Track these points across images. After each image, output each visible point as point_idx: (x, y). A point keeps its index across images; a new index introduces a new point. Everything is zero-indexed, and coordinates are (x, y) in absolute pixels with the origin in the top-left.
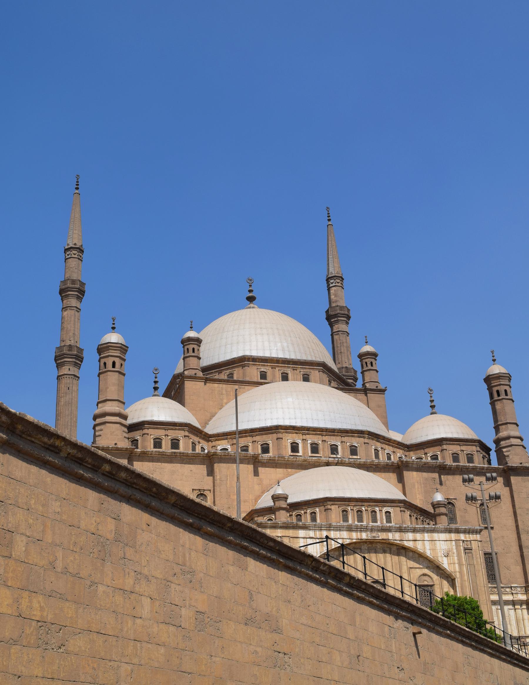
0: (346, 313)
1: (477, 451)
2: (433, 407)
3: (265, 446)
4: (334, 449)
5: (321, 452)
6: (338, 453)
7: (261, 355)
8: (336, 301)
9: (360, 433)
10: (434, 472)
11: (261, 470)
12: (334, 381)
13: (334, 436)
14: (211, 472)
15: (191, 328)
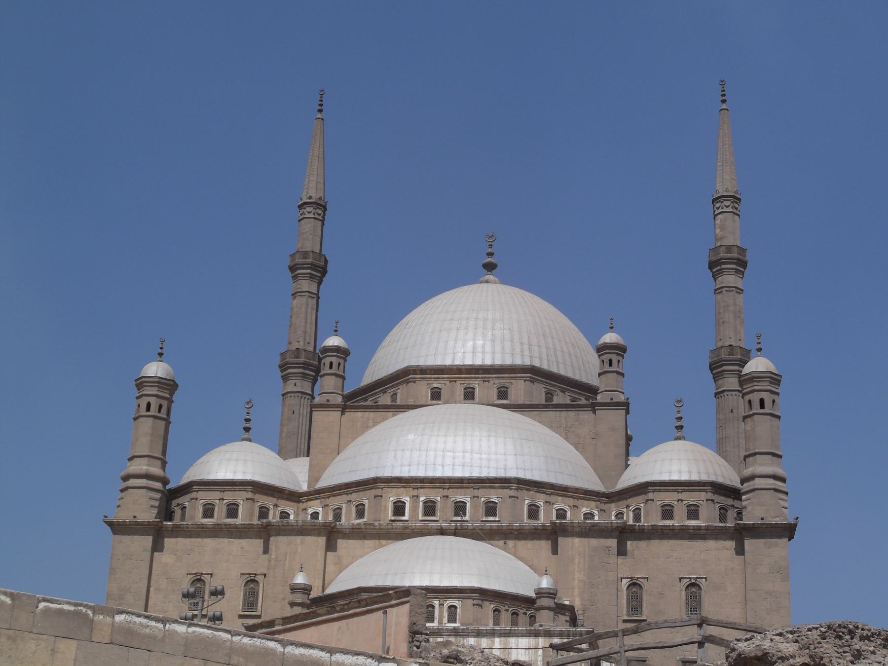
0: (736, 255)
1: (707, 500)
2: (680, 428)
3: (361, 507)
4: (460, 508)
5: (438, 513)
6: (465, 514)
7: (439, 363)
8: (721, 239)
9: (504, 482)
10: (611, 537)
11: (341, 543)
12: (564, 392)
13: (462, 488)
14: (266, 551)
15: (336, 331)
